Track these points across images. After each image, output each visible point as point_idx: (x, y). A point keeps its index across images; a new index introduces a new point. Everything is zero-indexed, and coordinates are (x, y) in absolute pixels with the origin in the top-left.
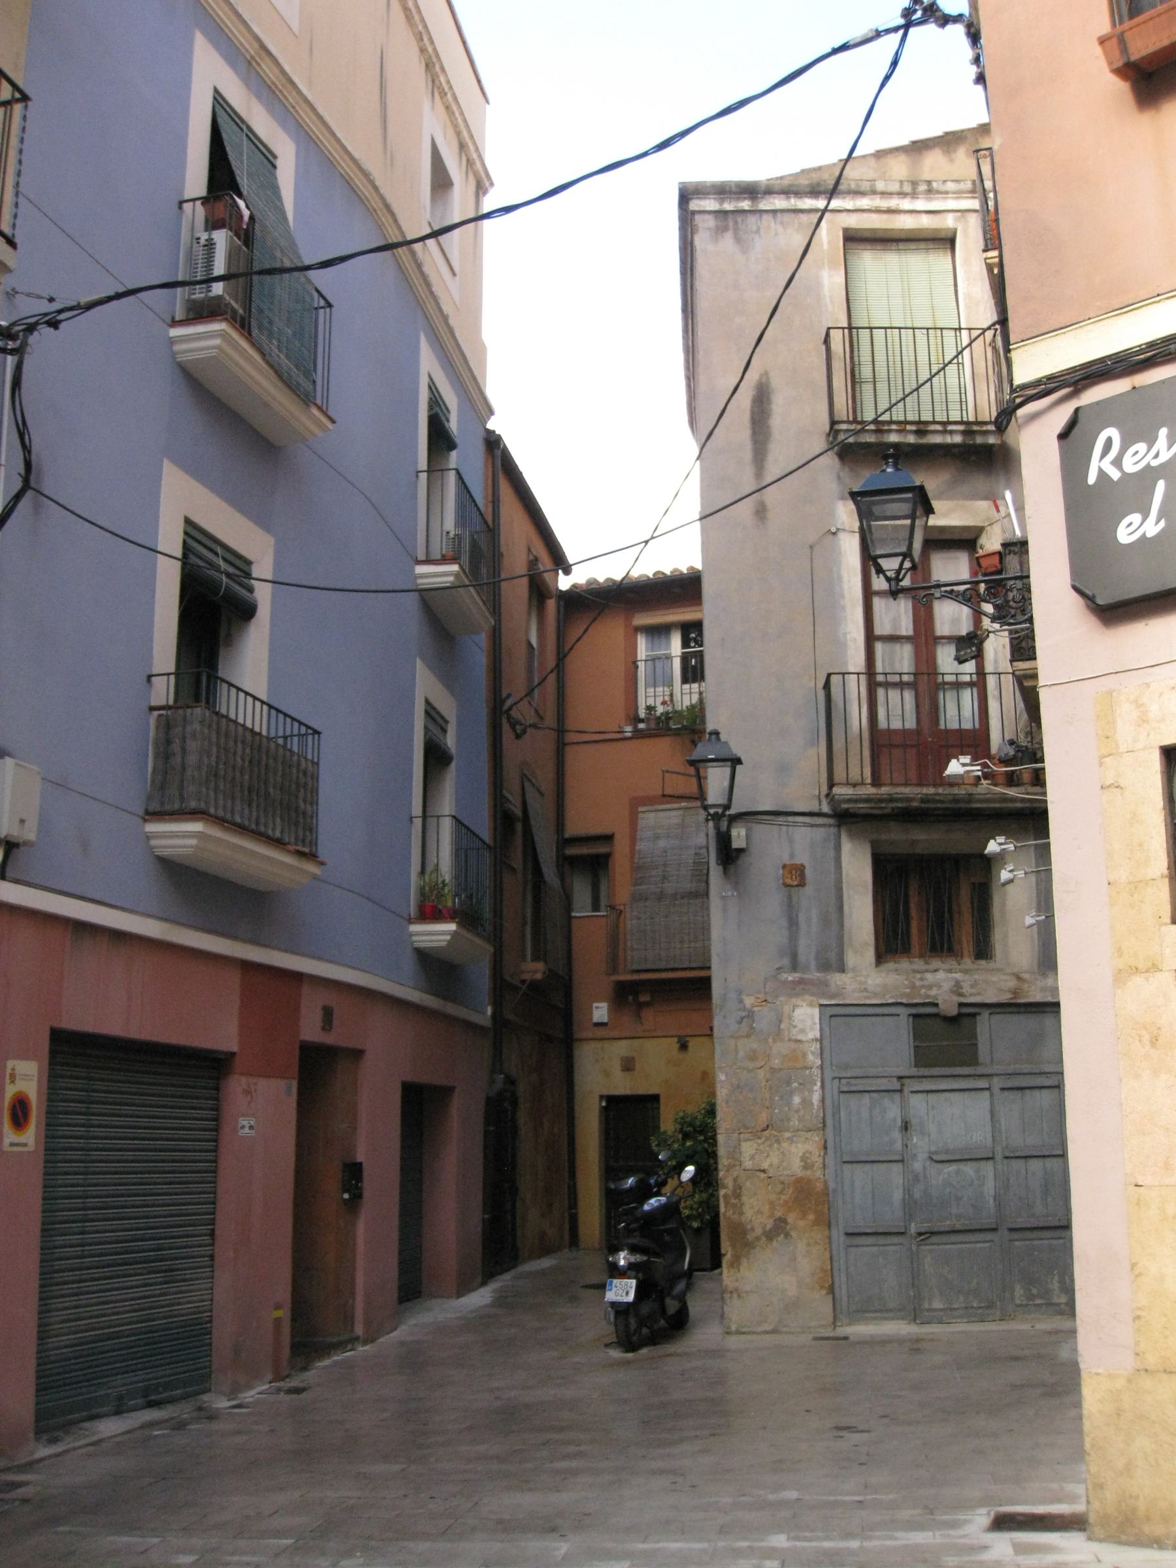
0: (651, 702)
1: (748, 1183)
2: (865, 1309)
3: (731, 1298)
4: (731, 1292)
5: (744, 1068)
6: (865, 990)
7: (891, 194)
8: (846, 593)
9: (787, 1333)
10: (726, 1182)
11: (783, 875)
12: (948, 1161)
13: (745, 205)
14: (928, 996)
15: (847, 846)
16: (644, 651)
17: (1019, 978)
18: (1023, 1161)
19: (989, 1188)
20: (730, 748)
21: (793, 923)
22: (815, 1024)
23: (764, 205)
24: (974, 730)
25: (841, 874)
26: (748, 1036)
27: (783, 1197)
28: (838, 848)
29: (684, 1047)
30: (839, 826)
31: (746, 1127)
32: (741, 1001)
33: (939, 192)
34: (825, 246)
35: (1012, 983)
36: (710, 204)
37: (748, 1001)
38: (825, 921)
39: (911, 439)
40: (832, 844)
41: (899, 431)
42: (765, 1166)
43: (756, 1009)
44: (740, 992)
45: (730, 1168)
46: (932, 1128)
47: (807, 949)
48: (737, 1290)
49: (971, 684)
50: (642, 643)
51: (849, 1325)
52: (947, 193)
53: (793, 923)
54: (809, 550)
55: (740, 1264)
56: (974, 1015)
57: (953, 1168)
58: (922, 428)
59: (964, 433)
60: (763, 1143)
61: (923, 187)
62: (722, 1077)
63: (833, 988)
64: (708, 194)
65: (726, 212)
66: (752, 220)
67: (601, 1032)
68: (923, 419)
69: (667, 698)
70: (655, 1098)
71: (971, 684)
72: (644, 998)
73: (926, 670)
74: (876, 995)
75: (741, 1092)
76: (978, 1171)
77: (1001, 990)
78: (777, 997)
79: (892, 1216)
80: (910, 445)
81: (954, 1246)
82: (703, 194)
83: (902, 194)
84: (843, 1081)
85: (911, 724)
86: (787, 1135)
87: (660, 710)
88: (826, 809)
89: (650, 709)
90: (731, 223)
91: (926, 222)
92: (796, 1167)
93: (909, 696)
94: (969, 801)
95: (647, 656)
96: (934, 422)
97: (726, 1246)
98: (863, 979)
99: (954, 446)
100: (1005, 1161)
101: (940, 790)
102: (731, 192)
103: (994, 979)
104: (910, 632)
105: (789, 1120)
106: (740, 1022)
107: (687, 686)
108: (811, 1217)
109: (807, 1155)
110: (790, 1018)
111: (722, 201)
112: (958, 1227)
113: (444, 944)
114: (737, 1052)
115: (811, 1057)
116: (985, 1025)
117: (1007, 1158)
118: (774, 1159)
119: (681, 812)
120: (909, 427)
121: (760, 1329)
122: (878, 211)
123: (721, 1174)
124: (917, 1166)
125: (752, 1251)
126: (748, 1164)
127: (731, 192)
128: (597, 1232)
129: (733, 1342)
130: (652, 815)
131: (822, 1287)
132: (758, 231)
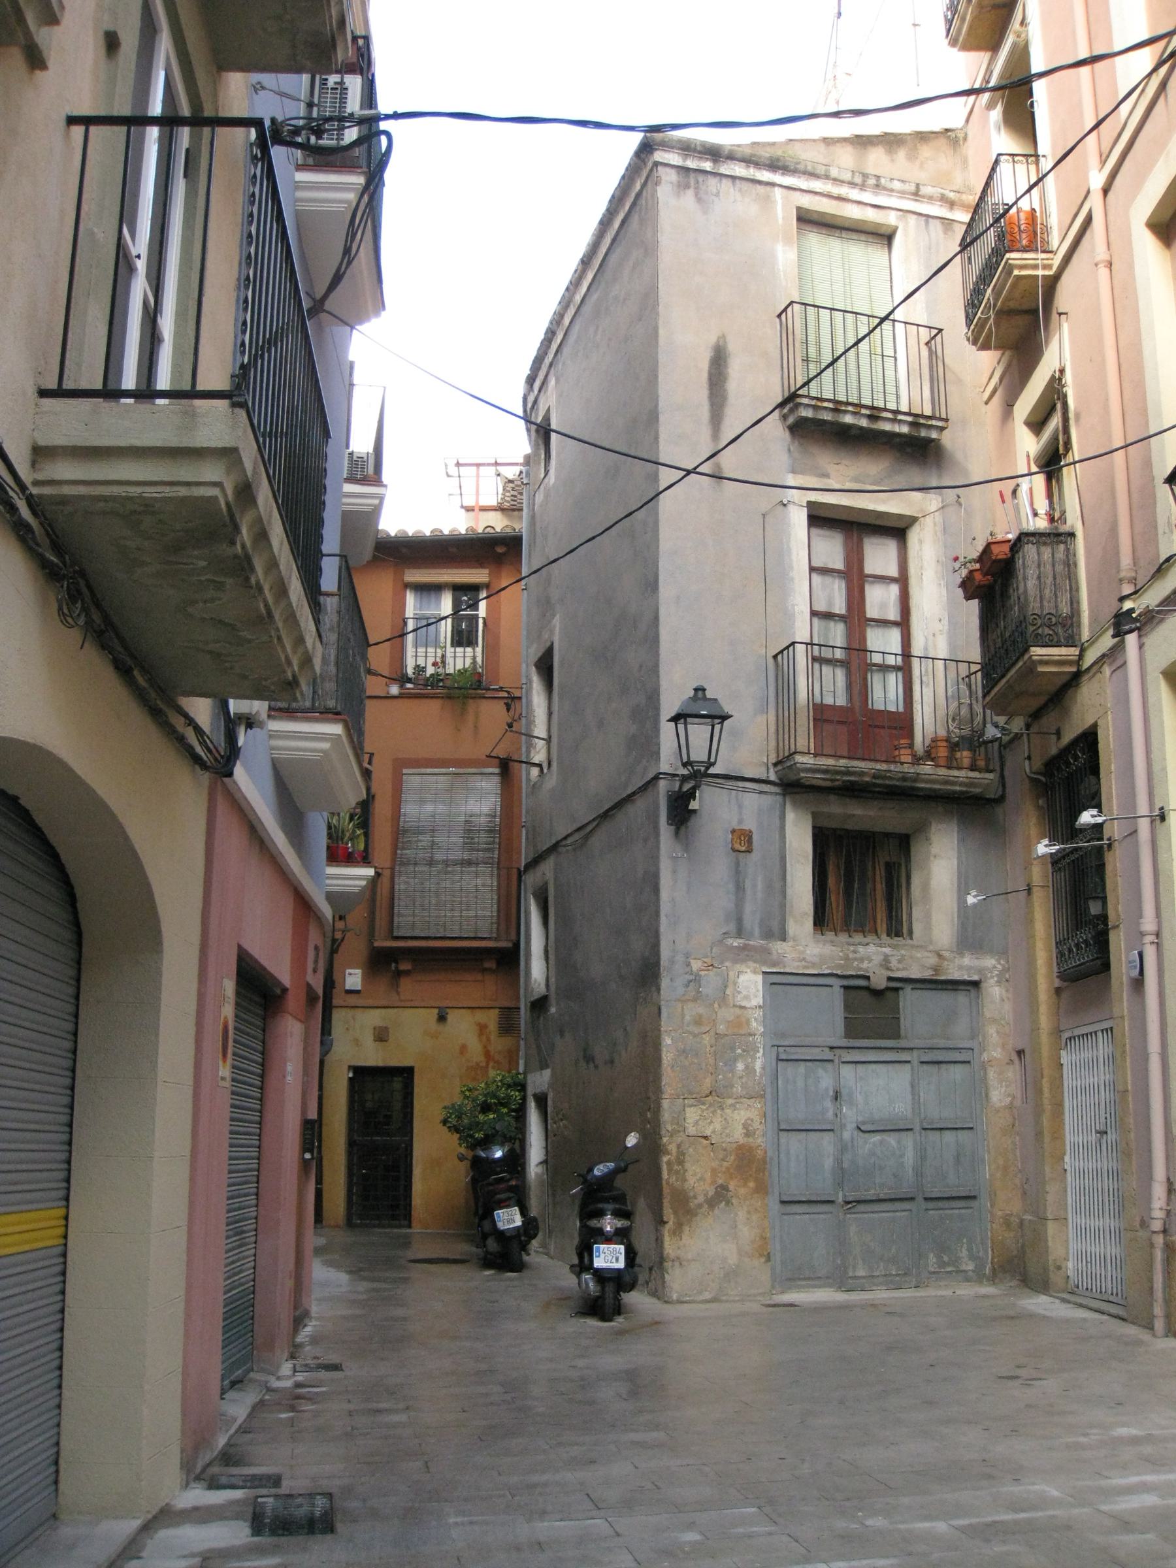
0: (421, 662)
1: (691, 1150)
2: (794, 1278)
3: (672, 1266)
4: (673, 1261)
5: (690, 1033)
6: (804, 959)
7: (843, 182)
8: (795, 565)
9: (727, 1301)
10: (670, 1147)
11: (732, 839)
12: (873, 1131)
13: (707, 166)
14: (860, 969)
15: (790, 816)
16: (412, 608)
17: (940, 956)
18: (938, 1133)
19: (909, 1157)
20: (721, 708)
21: (740, 888)
22: (758, 991)
23: (725, 169)
24: (897, 713)
25: (785, 843)
26: (695, 1000)
27: (725, 1164)
28: (783, 817)
29: (442, 1018)
30: (784, 795)
31: (691, 1093)
32: (688, 965)
33: (885, 189)
34: (780, 221)
35: (933, 960)
36: (674, 158)
37: (696, 965)
38: (769, 887)
39: (864, 423)
40: (778, 813)
41: (854, 413)
42: (708, 1133)
43: (702, 973)
44: (687, 955)
45: (672, 1134)
46: (860, 1099)
47: (751, 919)
48: (678, 1258)
49: (896, 668)
50: (410, 599)
51: (782, 1292)
52: (892, 190)
53: (740, 888)
54: (761, 517)
55: (681, 1232)
56: (897, 990)
57: (877, 1138)
58: (875, 414)
59: (911, 424)
60: (707, 1109)
61: (872, 181)
62: (669, 1041)
63: (775, 956)
64: (673, 148)
65: (688, 170)
66: (712, 182)
67: (352, 1000)
68: (876, 404)
69: (438, 660)
70: (407, 1073)
71: (896, 668)
72: (405, 966)
73: (857, 649)
74: (814, 965)
75: (686, 1058)
76: (899, 1142)
77: (923, 966)
78: (722, 962)
79: (823, 1185)
80: (861, 428)
81: (876, 1215)
82: (668, 147)
83: (852, 184)
84: (781, 1049)
85: (841, 701)
86: (730, 1101)
87: (430, 670)
88: (773, 777)
89: (419, 669)
90: (692, 182)
91: (871, 215)
92: (738, 1134)
93: (840, 674)
94: (915, 781)
95: (415, 614)
96: (886, 410)
97: (668, 1213)
98: (801, 948)
99: (899, 435)
100: (923, 1132)
101: (892, 767)
102: (695, 150)
103: (919, 955)
104: (843, 611)
105: (732, 1086)
106: (687, 986)
107: (460, 650)
108: (752, 1184)
109: (749, 1122)
110: (735, 983)
111: (686, 157)
112: (882, 1196)
113: (356, 890)
114: (683, 1016)
115: (754, 1024)
116: (909, 999)
117: (925, 1129)
118: (717, 1125)
119: (449, 777)
120: (864, 411)
121: (701, 1298)
122: (829, 196)
123: (665, 1140)
124: (846, 1135)
125: (694, 1219)
126: (691, 1130)
127: (695, 150)
128: (342, 1210)
129: (671, 1311)
130: (417, 778)
131: (761, 1255)
132: (717, 195)
